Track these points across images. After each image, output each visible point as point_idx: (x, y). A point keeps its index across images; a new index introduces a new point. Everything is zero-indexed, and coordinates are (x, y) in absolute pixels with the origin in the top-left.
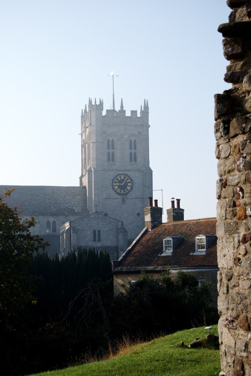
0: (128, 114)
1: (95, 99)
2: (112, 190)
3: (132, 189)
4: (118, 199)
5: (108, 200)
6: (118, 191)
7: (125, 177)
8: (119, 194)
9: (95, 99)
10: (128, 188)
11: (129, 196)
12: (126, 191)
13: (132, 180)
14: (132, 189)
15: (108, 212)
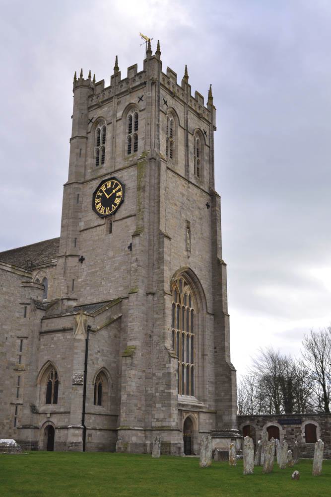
0: (124, 75)
1: (75, 74)
2: (93, 213)
3: (122, 202)
4: (101, 227)
5: (85, 232)
6: (102, 212)
7: (112, 183)
8: (102, 217)
9: (75, 74)
10: (117, 201)
11: (118, 216)
12: (114, 208)
13: (123, 186)
14: (122, 202)
15: (84, 255)
